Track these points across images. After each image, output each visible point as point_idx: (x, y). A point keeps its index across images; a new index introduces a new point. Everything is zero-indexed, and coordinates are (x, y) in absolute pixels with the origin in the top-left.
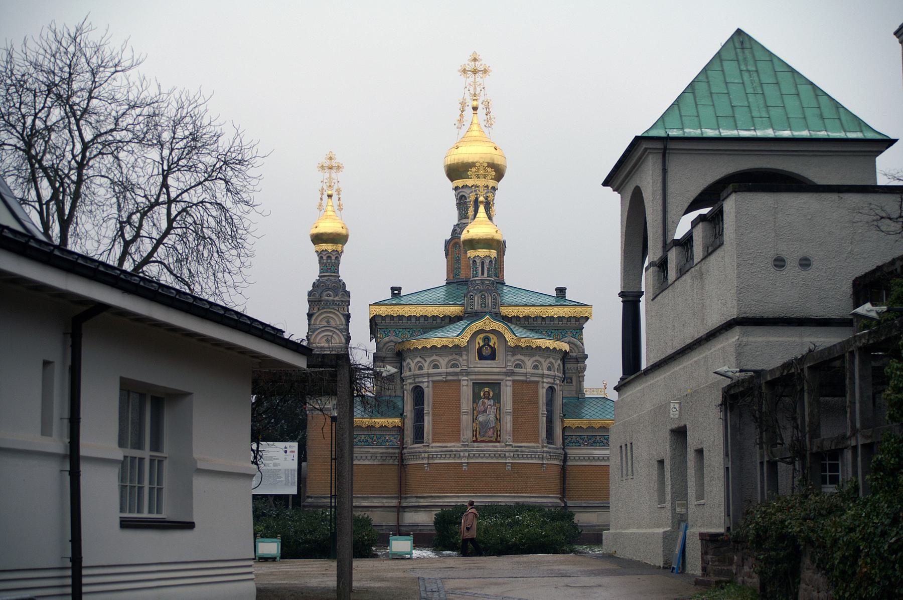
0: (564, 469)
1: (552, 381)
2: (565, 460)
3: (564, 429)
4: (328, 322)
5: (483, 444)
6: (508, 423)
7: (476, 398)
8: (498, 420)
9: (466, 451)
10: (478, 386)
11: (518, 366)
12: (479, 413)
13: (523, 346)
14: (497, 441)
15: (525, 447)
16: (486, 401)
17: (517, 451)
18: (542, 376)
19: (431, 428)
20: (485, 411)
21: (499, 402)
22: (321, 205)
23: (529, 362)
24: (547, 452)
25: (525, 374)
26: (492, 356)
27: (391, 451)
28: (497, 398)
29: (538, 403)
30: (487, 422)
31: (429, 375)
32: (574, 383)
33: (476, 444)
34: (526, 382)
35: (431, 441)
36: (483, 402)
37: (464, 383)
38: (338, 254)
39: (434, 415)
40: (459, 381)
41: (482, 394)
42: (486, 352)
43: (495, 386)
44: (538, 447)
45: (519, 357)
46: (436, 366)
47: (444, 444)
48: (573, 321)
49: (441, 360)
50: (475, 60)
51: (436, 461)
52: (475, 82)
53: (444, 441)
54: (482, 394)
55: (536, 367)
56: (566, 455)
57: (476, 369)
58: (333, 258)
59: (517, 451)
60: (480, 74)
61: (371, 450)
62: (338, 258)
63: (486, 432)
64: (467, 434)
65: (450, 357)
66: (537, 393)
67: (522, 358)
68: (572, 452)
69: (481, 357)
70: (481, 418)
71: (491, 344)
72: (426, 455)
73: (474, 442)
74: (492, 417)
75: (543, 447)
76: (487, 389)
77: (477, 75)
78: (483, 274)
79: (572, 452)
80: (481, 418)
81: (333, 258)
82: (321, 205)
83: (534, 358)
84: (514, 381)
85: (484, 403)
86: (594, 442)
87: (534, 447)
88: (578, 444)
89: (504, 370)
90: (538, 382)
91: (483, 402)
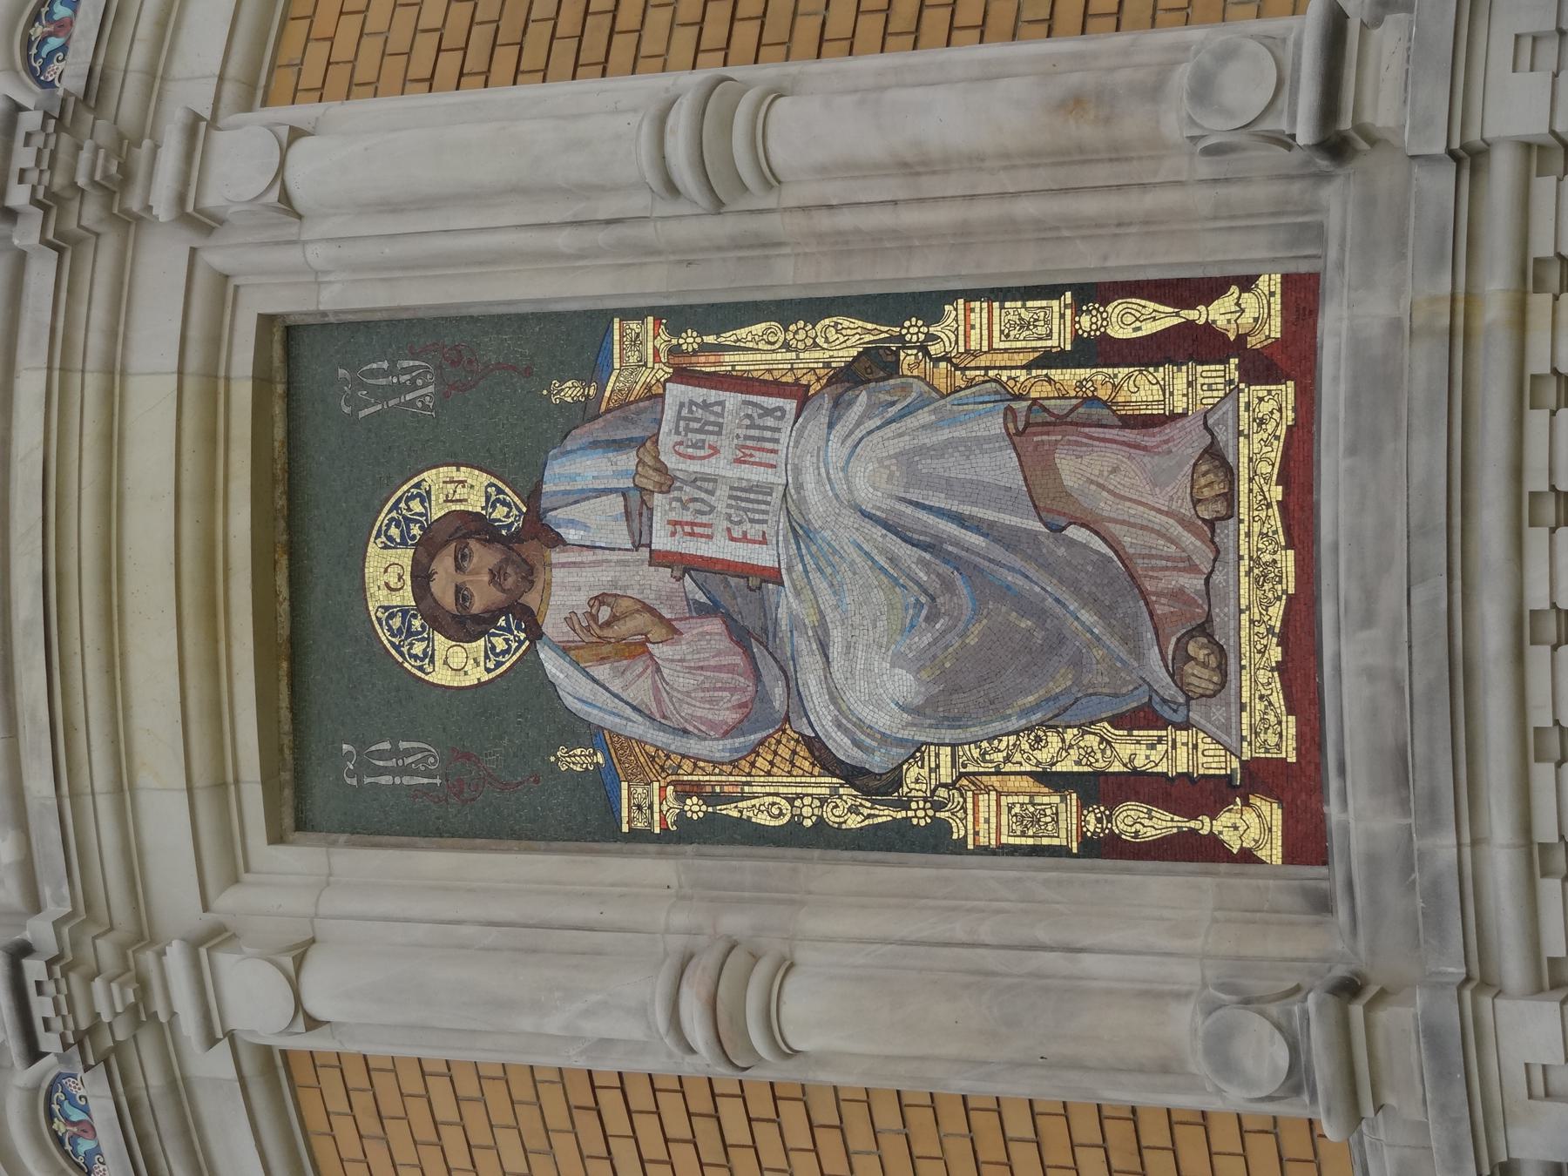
5: (1349, 655)
7: (517, 781)
10: (328, 742)
12: (770, 723)
14: (1287, 360)
16: (566, 592)
20: (737, 603)
21: (582, 337)
28: (515, 375)
30: (941, 563)
33: (1357, 814)
40: (277, 1073)
41: (457, 665)
43: (319, 414)
54: (457, 665)
63: (1123, 580)
73: (1307, 842)
74: (847, 468)
76: (386, 574)
80: (868, 682)
85: (613, 634)
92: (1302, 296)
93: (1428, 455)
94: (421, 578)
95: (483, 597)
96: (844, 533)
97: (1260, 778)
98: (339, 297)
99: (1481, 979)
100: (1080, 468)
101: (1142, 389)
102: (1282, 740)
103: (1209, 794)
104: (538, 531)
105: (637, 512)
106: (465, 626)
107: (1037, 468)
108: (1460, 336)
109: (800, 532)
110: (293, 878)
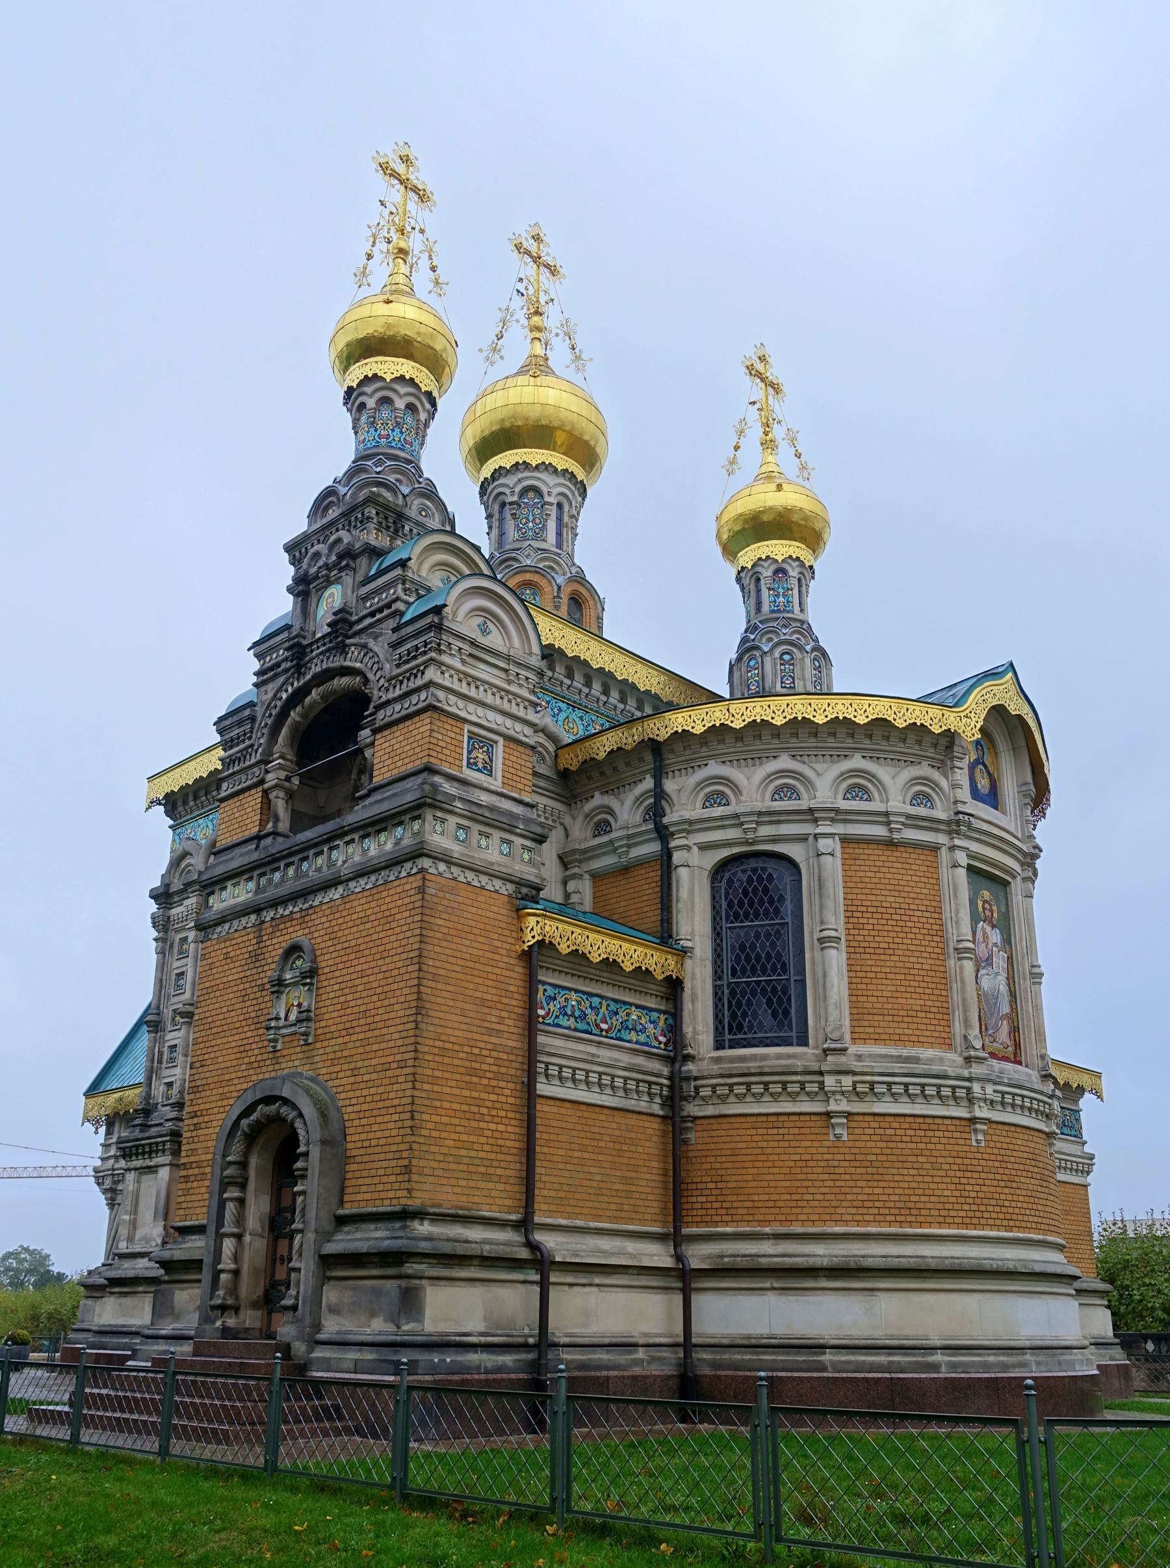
19: (845, 992)
20: (989, 961)
27: (640, 1061)
31: (838, 816)
39: (853, 952)
46: (857, 791)
47: (904, 1052)
49: (883, 772)
51: (879, 1108)
53: (899, 1041)
65: (915, 771)
72: (847, 1081)
92: (1020, 1063)
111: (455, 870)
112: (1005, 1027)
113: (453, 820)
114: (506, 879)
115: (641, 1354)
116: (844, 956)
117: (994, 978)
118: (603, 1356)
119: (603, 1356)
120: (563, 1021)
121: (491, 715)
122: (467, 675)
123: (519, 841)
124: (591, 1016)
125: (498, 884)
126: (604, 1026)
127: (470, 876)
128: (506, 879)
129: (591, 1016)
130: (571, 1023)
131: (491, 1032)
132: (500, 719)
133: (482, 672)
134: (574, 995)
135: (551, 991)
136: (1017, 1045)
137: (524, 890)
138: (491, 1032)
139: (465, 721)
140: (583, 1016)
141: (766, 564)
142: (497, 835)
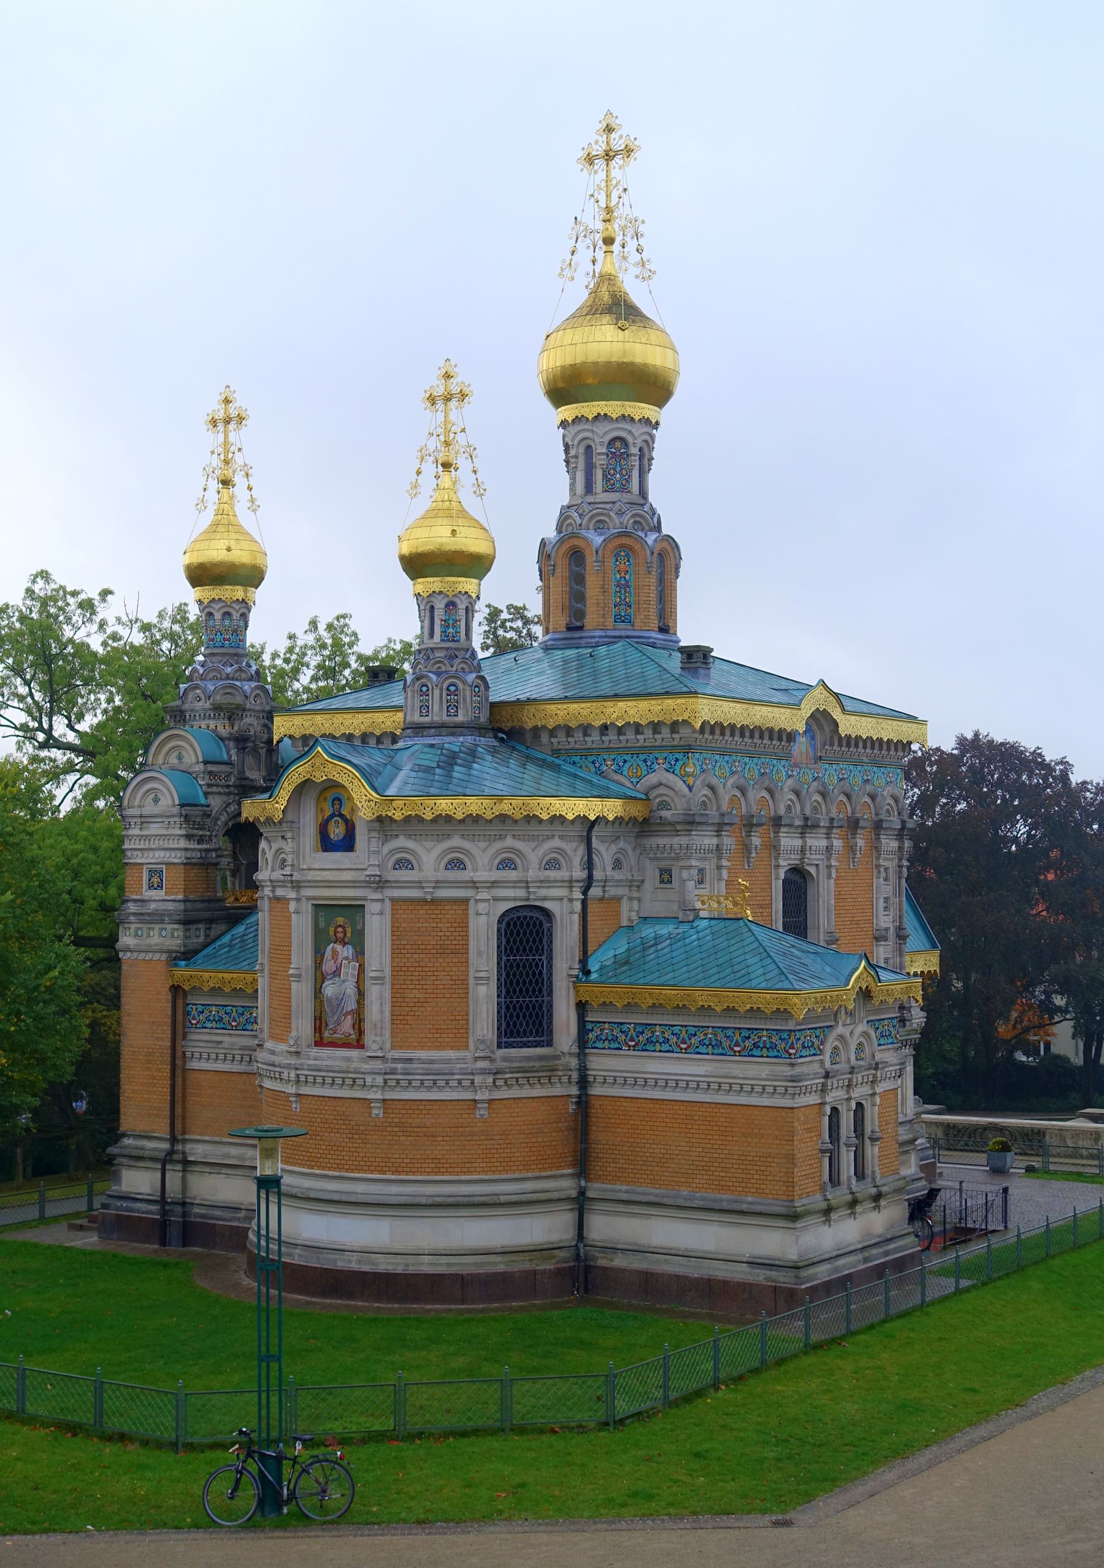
0: (584, 1102)
1: (521, 893)
2: (584, 1082)
3: (581, 1007)
4: (180, 758)
6: (378, 1006)
8: (361, 994)
9: (288, 1066)
11: (403, 864)
13: (398, 816)
14: (360, 1045)
15: (421, 1061)
16: (338, 947)
17: (393, 1072)
18: (474, 885)
20: (337, 973)
22: (415, 486)
23: (430, 858)
24: (483, 1072)
25: (419, 884)
26: (348, 844)
29: (462, 951)
30: (341, 1000)
32: (676, 883)
33: (315, 1051)
34: (425, 901)
35: (266, 1035)
36: (334, 951)
37: (292, 906)
38: (245, 606)
42: (337, 831)
44: (463, 1060)
45: (402, 842)
48: (666, 732)
50: (609, 129)
52: (608, 180)
55: (457, 864)
56: (583, 1070)
57: (311, 876)
58: (218, 616)
59: (393, 1072)
60: (618, 161)
61: (226, 1039)
62: (244, 617)
64: (303, 1027)
66: (464, 926)
67: (410, 844)
68: (601, 1063)
69: (327, 844)
70: (330, 989)
71: (345, 811)
74: (350, 989)
75: (476, 1059)
76: (340, 920)
77: (613, 163)
78: (432, 635)
79: (601, 1063)
81: (218, 616)
82: (252, 500)
83: (447, 844)
84: (393, 900)
85: (335, 953)
86: (649, 1041)
87: (449, 1061)
88: (615, 1044)
89: (361, 876)
90: (466, 901)
91: (334, 951)
93: (336, 1069)
94: (340, 926)
95: (338, 935)
96: (343, 987)
97: (322, 1038)
98: (367, 916)
99: (297, 1069)
100: (349, 1017)
101: (357, 1027)
102: (325, 1041)
103: (320, 1033)
104: (345, 944)
105: (346, 958)
106: (335, 932)
107: (348, 1013)
108: (348, 1072)
109: (344, 981)
110: (307, 908)
111: (135, 954)
112: (349, 1021)
113: (133, 926)
114: (161, 951)
115: (243, 1214)
116: (267, 979)
117: (341, 985)
118: (217, 1213)
119: (217, 1213)
120: (209, 1025)
121: (157, 854)
122: (142, 836)
123: (169, 927)
124: (226, 1018)
125: (158, 955)
126: (234, 1024)
127: (142, 956)
128: (161, 951)
129: (226, 1018)
130: (214, 1025)
131: (158, 1039)
132: (162, 854)
133: (154, 829)
134: (214, 1008)
135: (200, 1008)
136: (361, 1033)
137: (174, 955)
138: (158, 1039)
139: (142, 864)
140: (221, 1020)
141: (440, 597)
142: (157, 927)
